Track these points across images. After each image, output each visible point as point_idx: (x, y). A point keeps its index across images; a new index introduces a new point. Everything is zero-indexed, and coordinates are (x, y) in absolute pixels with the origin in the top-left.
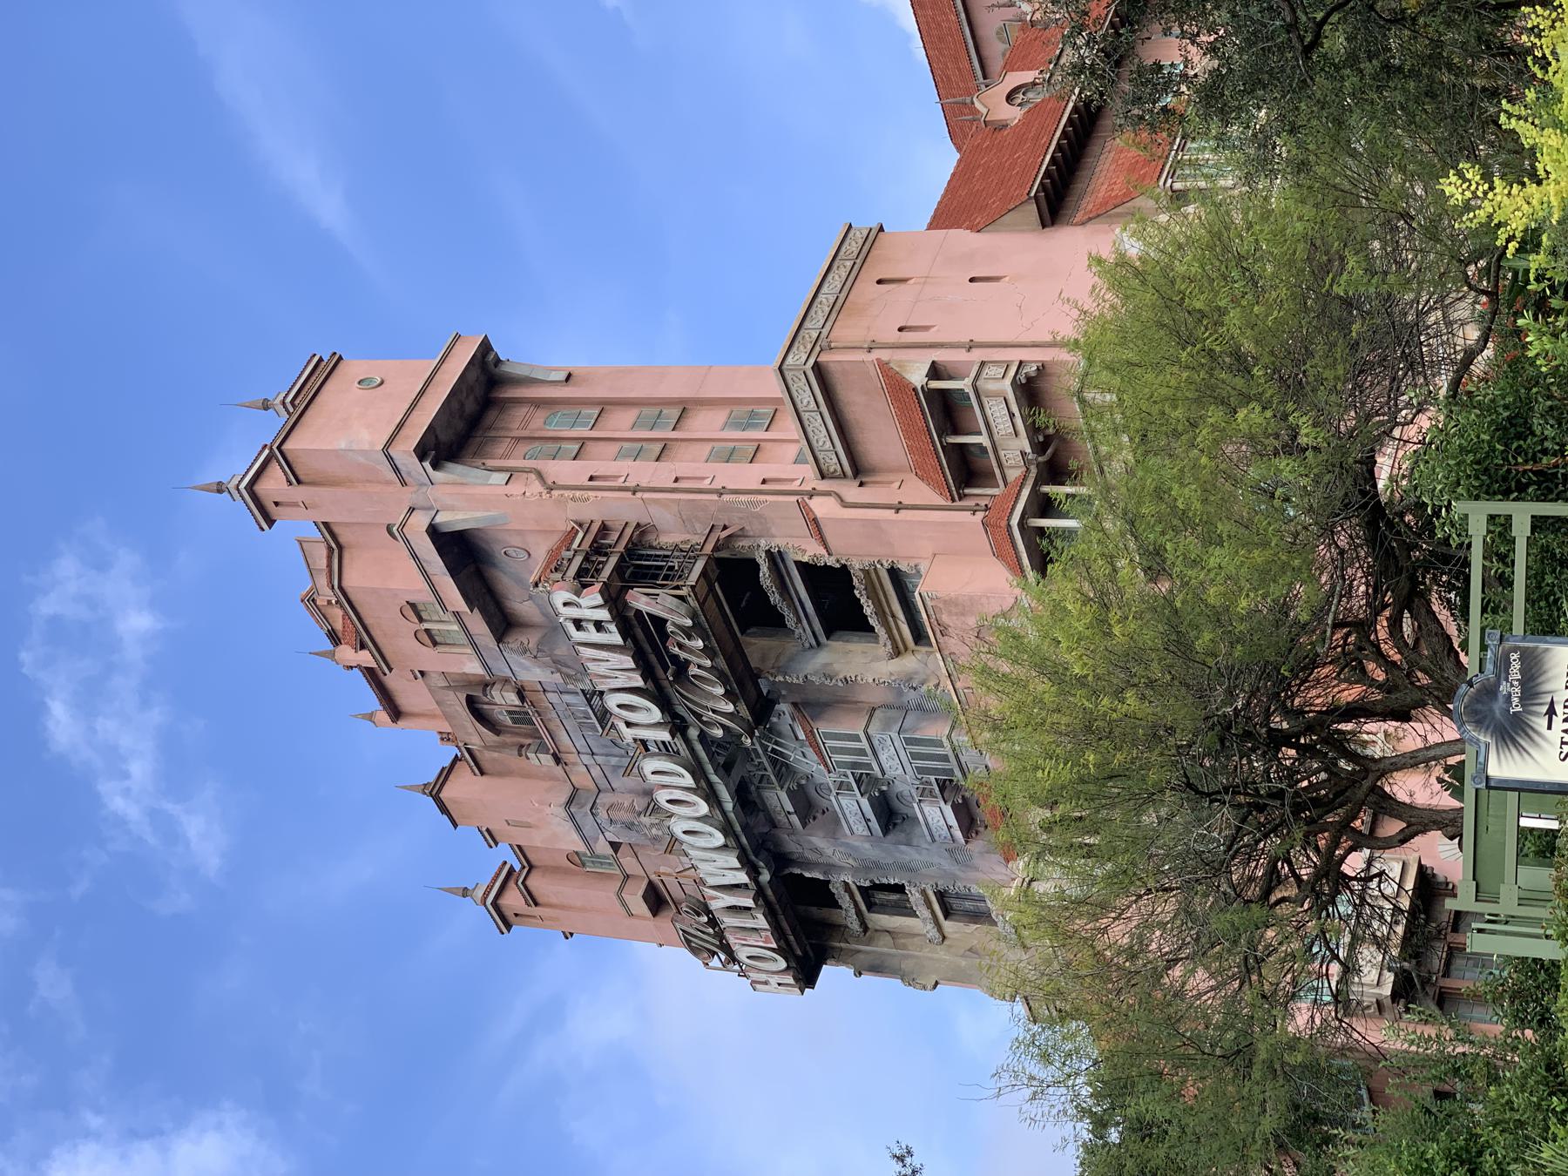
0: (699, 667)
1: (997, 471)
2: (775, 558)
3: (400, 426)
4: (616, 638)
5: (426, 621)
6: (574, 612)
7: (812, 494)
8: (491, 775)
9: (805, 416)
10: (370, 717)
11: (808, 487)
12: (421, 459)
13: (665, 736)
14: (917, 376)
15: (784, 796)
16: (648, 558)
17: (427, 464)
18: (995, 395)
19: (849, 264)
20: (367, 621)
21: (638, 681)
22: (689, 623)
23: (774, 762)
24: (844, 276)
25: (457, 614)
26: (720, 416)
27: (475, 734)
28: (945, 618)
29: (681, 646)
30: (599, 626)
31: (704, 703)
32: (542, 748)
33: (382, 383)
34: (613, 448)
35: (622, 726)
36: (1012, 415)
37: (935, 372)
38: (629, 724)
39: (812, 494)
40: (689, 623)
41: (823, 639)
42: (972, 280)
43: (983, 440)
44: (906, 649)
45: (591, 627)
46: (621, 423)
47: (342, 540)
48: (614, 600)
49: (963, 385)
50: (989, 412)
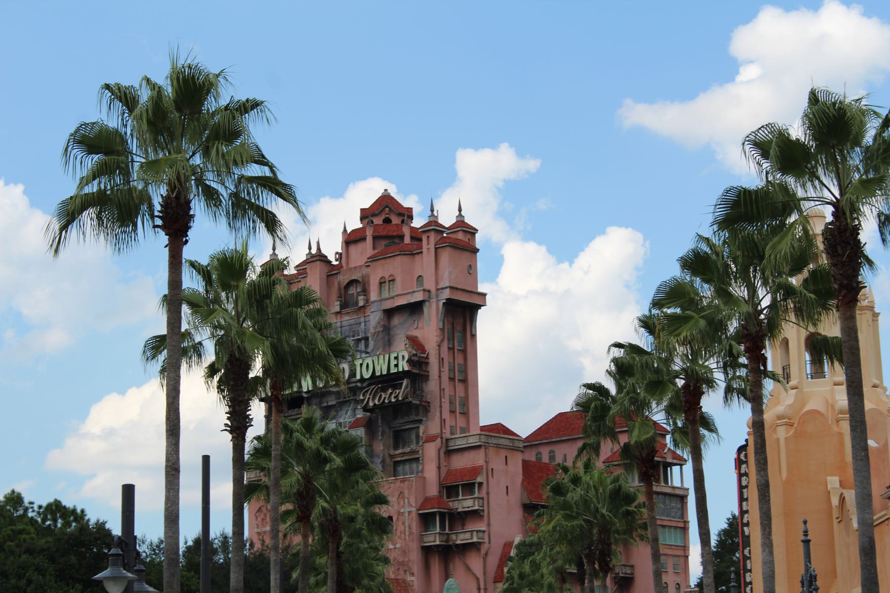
0: (385, 398)
1: (451, 499)
2: (420, 421)
3: (457, 289)
4: (392, 371)
5: (389, 283)
6: (400, 358)
7: (442, 438)
8: (327, 279)
9: (465, 439)
10: (345, 230)
11: (444, 436)
12: (447, 299)
13: (358, 377)
14: (479, 479)
15: (334, 403)
16: (419, 384)
17: (444, 301)
18: (474, 503)
19: (511, 445)
20: (388, 260)
21: (378, 374)
22: (400, 399)
23: (348, 401)
24: (508, 444)
25: (393, 298)
26: (463, 395)
27: (344, 279)
28: (406, 483)
29: (391, 394)
30: (396, 366)
31: (372, 395)
32: (343, 306)
33: (470, 273)
34: (452, 361)
35: (361, 361)
36: (469, 507)
37: (480, 484)
38: (361, 365)
39: (442, 438)
40: (400, 399)
41: (392, 430)
42: (507, 487)
43: (460, 497)
44: (392, 458)
45: (396, 363)
46: (459, 360)
47: (416, 256)
48: (404, 374)
49: (476, 495)
50: (469, 500)
